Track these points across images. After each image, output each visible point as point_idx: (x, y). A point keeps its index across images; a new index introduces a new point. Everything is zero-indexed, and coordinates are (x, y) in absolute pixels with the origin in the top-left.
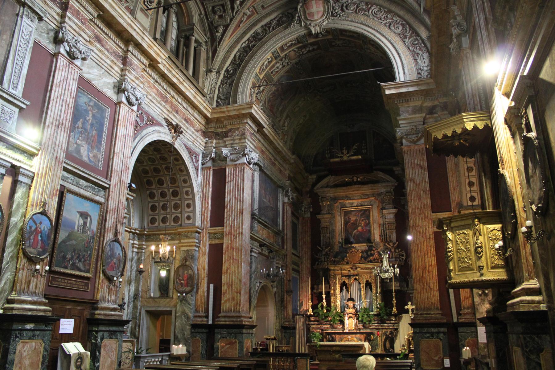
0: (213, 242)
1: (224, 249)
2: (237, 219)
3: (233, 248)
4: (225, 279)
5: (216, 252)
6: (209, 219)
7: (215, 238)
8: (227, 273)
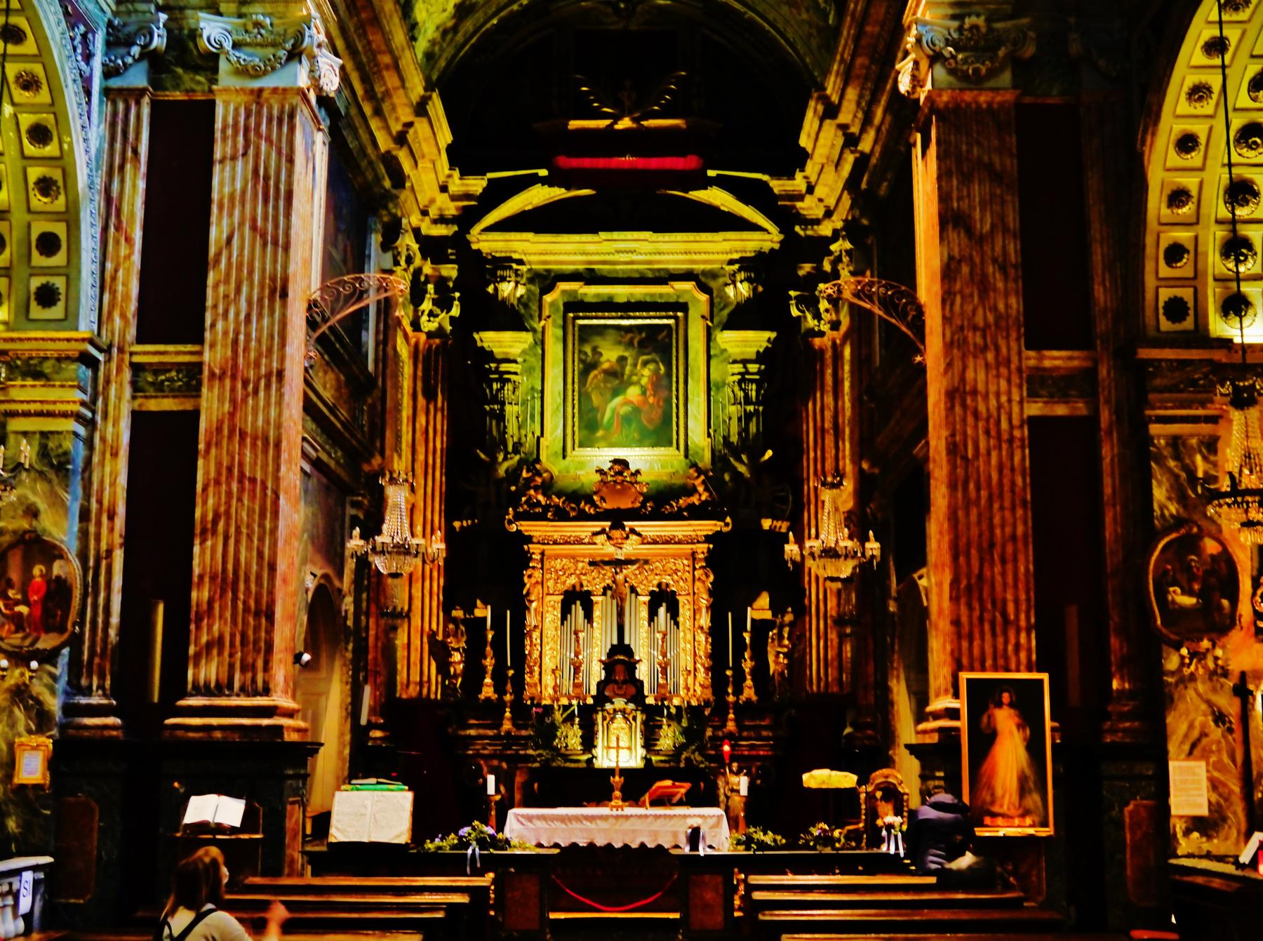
0: (153, 405)
1: (202, 437)
2: (260, 315)
3: (243, 435)
4: (203, 556)
5: (164, 451)
6: (133, 306)
7: (159, 388)
8: (214, 532)
